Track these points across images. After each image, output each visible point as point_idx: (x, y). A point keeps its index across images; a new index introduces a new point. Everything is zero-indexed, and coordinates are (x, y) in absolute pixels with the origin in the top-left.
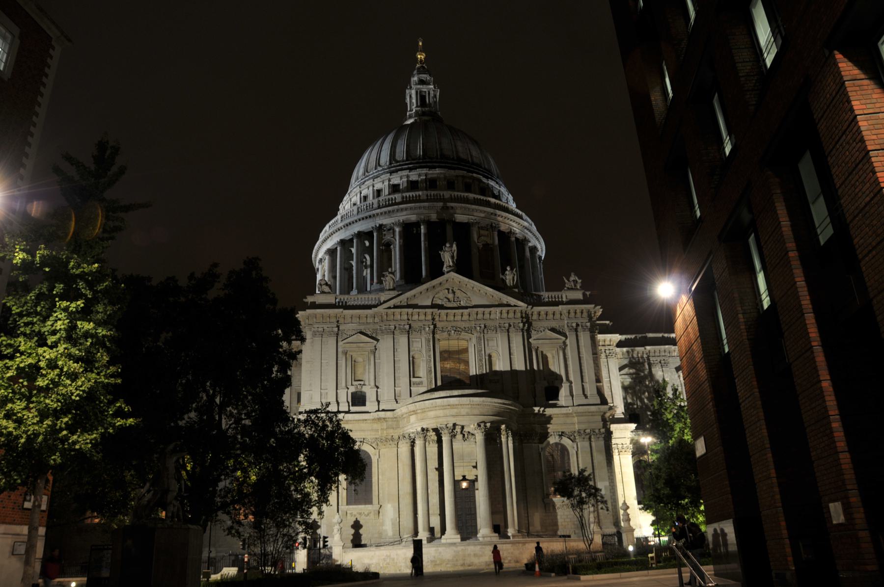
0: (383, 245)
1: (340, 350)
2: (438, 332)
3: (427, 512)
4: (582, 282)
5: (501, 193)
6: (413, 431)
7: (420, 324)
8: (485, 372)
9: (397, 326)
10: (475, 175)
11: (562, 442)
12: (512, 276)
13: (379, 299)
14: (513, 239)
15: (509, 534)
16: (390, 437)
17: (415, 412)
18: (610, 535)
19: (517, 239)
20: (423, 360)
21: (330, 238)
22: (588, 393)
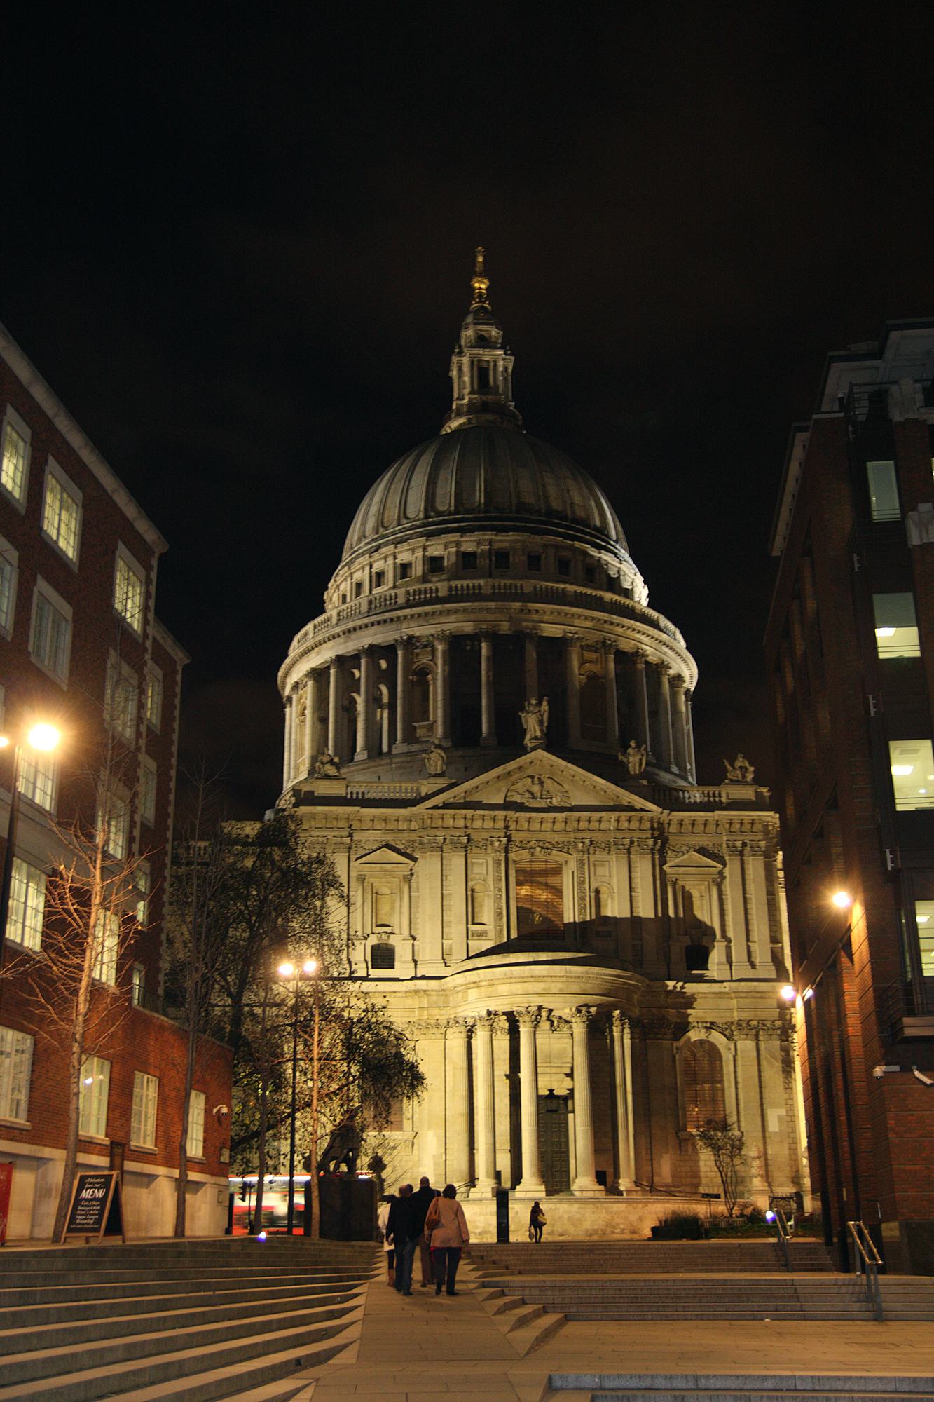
0: (415, 673)
1: (353, 874)
2: (515, 849)
3: (492, 1147)
4: (754, 772)
5: (622, 573)
6: (473, 1014)
7: (485, 835)
8: (588, 919)
9: (448, 838)
10: (577, 544)
11: (711, 1039)
12: (639, 757)
13: (418, 789)
14: (641, 666)
15: (622, 1188)
16: (433, 1022)
17: (476, 984)
18: (783, 1198)
19: (647, 663)
20: (488, 896)
21: (316, 650)
22: (757, 959)
